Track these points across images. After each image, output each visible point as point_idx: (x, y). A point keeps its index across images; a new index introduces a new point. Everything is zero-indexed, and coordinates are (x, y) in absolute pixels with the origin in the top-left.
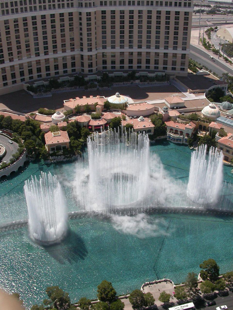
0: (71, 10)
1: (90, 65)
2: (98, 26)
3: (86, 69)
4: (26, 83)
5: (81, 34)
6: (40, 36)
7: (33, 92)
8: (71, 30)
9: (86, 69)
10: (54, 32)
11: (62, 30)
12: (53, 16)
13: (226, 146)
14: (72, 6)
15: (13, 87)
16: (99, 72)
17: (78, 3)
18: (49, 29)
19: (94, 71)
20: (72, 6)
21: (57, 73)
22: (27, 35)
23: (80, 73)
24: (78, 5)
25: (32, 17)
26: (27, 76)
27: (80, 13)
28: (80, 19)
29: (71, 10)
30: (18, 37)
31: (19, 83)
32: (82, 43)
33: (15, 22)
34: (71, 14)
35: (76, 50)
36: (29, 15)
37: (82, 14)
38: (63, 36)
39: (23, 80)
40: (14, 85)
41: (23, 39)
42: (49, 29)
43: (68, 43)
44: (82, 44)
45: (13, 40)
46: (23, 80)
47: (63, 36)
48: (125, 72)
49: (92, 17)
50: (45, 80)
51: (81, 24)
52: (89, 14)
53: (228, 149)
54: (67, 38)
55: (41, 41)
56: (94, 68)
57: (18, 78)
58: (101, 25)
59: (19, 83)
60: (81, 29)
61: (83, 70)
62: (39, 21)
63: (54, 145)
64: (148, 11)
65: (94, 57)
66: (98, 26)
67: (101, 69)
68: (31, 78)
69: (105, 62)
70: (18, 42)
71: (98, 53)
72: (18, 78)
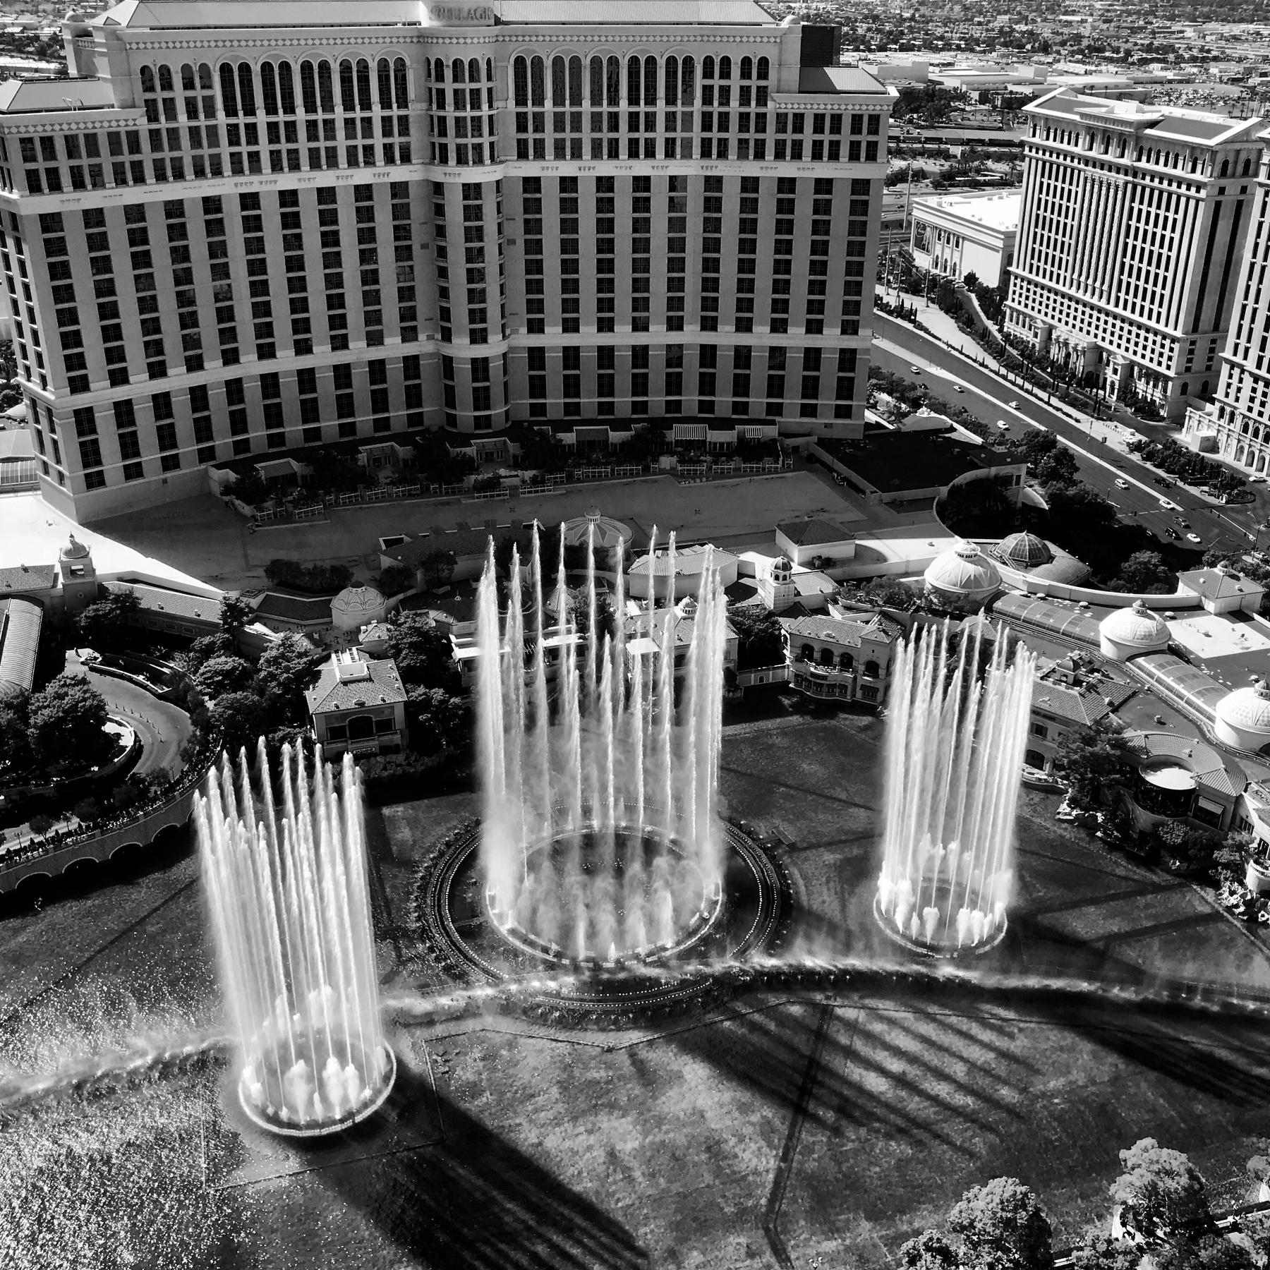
0: (399, 173)
1: (482, 399)
2: (512, 242)
3: (466, 413)
4: (219, 467)
5: (443, 273)
7: (249, 504)
8: (403, 253)
10: (332, 260)
15: (165, 481)
16: (517, 424)
17: (429, 147)
20: (406, 158)
22: (221, 271)
23: (441, 428)
24: (429, 153)
25: (242, 196)
26: (223, 441)
27: (438, 188)
28: (440, 210)
29: (399, 173)
30: (183, 277)
34: (399, 189)
35: (422, 337)
36: (227, 187)
38: (370, 277)
39: (206, 455)
40: (169, 475)
44: (445, 314)
46: (206, 455)
47: (370, 277)
49: (488, 203)
50: (294, 454)
51: (441, 231)
52: (472, 191)
56: (497, 411)
57: (187, 447)
60: (442, 253)
61: (452, 420)
62: (271, 213)
63: (345, 714)
64: (707, 179)
65: (495, 366)
66: (512, 242)
67: (525, 415)
68: (241, 447)
69: (538, 387)
70: (185, 299)
71: (512, 349)
72: (187, 447)
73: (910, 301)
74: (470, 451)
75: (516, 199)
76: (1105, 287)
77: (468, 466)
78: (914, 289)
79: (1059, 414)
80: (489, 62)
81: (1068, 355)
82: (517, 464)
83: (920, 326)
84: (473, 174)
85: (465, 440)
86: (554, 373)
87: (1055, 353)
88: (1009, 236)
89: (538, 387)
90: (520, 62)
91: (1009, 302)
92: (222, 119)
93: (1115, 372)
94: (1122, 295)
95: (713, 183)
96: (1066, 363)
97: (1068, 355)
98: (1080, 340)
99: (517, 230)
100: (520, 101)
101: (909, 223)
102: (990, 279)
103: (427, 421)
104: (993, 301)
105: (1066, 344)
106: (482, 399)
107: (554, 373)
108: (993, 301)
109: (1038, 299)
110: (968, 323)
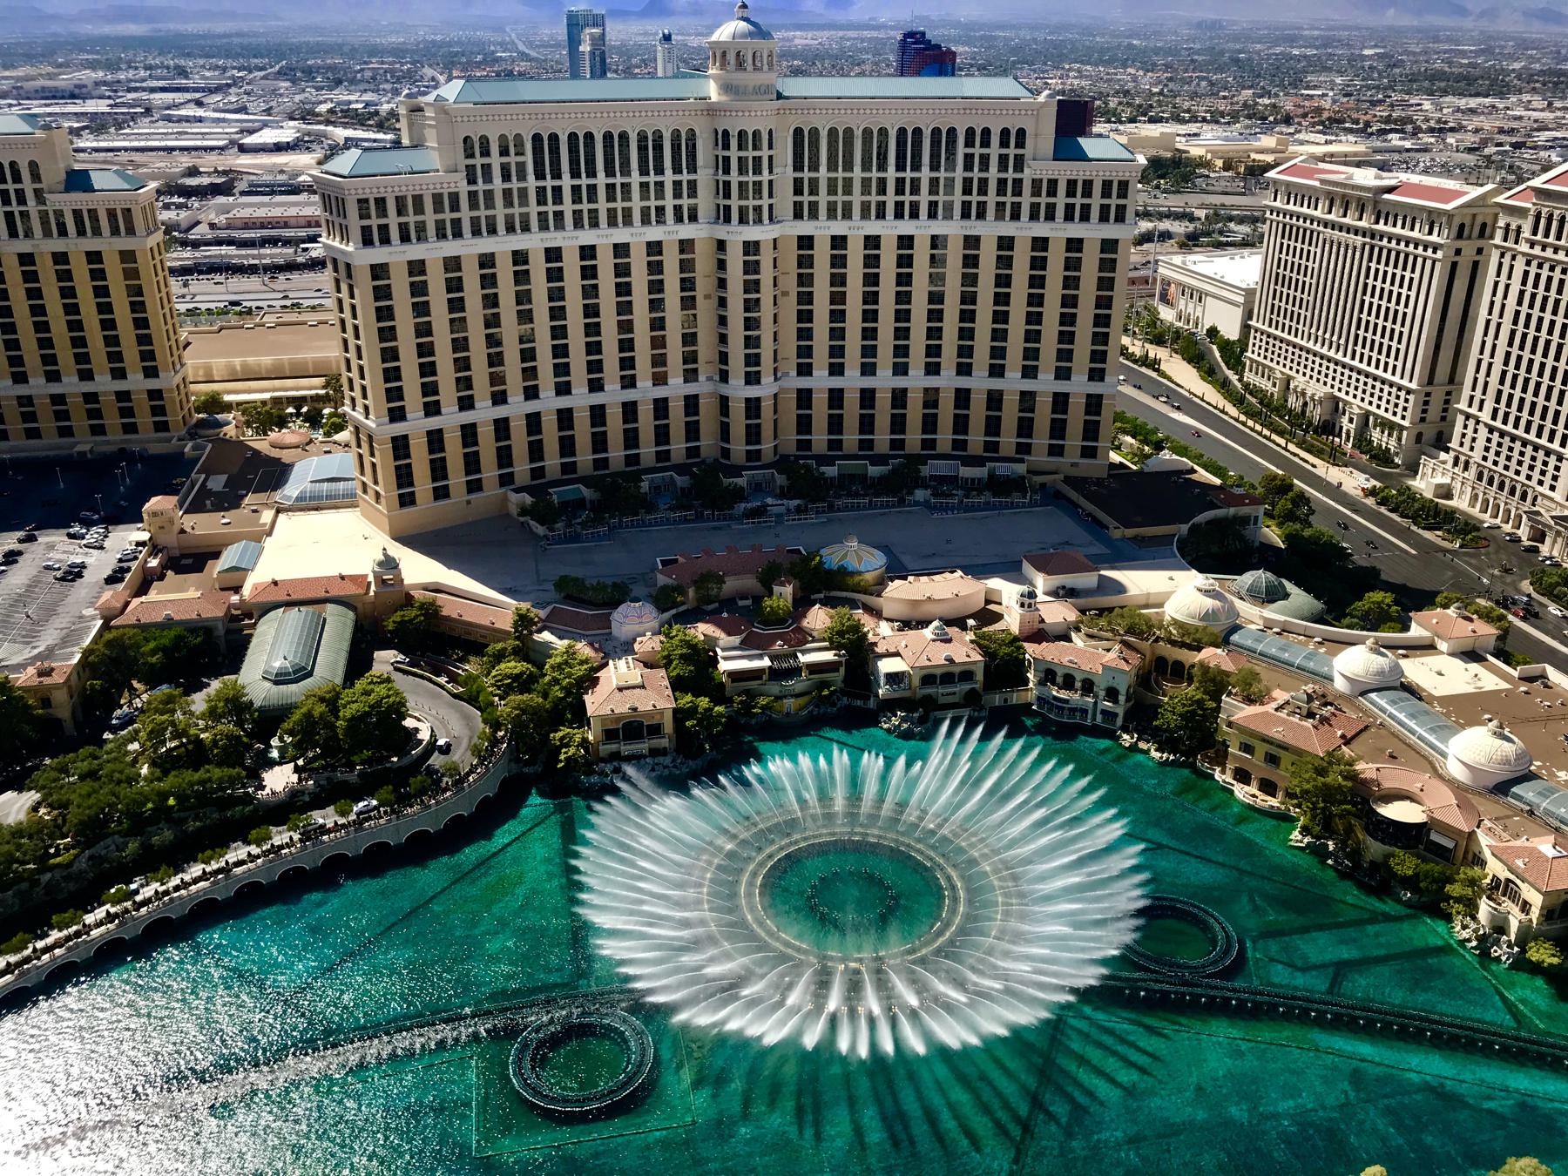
1: (753, 434)
2: (785, 294)
3: (739, 447)
4: (517, 491)
5: (723, 321)
6: (575, 321)
8: (688, 303)
9: (739, 447)
10: (625, 308)
11: (656, 305)
12: (621, 250)
13: (1266, 740)
14: (693, 218)
15: (469, 502)
16: (785, 458)
18: (607, 299)
20: (693, 218)
21: (632, 460)
22: (525, 317)
23: (716, 460)
24: (714, 213)
25: (547, 250)
26: (521, 467)
28: (722, 265)
29: (687, 231)
30: (492, 322)
31: (492, 490)
32: (726, 354)
33: (482, 266)
34: (686, 246)
35: (702, 378)
36: (534, 242)
38: (658, 324)
39: (506, 480)
40: (473, 496)
41: (510, 329)
42: (607, 299)
43: (675, 350)
44: (724, 358)
47: (658, 324)
49: (766, 259)
50: (584, 480)
51: (722, 284)
52: (751, 247)
53: (1274, 750)
54: (674, 334)
55: (576, 340)
56: (767, 446)
57: (490, 471)
59: (492, 490)
60: (722, 302)
61: (726, 453)
62: (572, 265)
64: (966, 238)
65: (767, 405)
66: (785, 294)
67: (792, 449)
68: (537, 473)
69: (804, 424)
70: (493, 341)
71: (782, 390)
72: (490, 471)
73: (1154, 351)
74: (741, 481)
75: (791, 254)
76: (1342, 341)
77: (738, 495)
78: (1159, 341)
79: (1296, 460)
80: (770, 132)
81: (1305, 404)
82: (784, 494)
84: (752, 233)
85: (737, 471)
86: (820, 411)
87: (1293, 402)
88: (1249, 293)
89: (804, 424)
90: (798, 132)
91: (1249, 354)
92: (532, 183)
93: (1351, 421)
94: (1359, 349)
95: (972, 242)
96: (1304, 412)
97: (1305, 404)
98: (1317, 390)
99: (790, 284)
100: (798, 167)
101: (1155, 280)
102: (1231, 332)
103: (704, 453)
104: (1234, 353)
105: (1303, 394)
106: (753, 434)
107: (820, 411)
108: (1234, 353)
110: (1209, 373)
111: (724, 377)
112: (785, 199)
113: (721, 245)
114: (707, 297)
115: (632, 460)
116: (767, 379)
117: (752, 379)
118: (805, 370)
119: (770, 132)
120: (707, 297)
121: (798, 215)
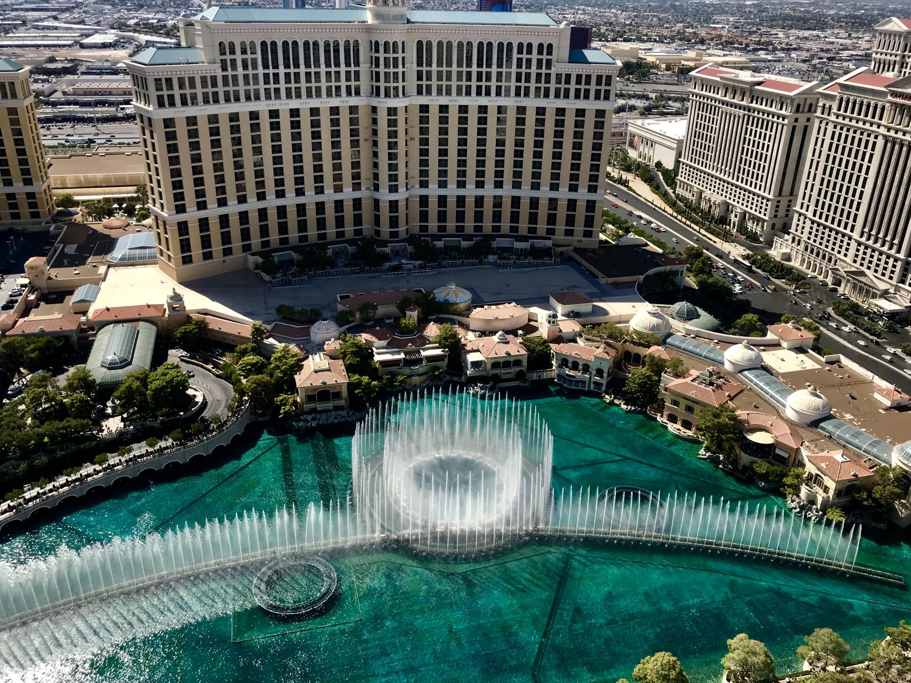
1: (394, 222)
2: (413, 139)
3: (385, 229)
4: (253, 254)
5: (375, 154)
6: (287, 153)
8: (355, 144)
9: (385, 229)
10: (317, 146)
12: (315, 112)
13: (686, 398)
14: (358, 93)
15: (224, 261)
16: (412, 236)
19: (403, 235)
20: (358, 93)
21: (322, 237)
22: (258, 151)
23: (372, 237)
24: (370, 91)
25: (270, 111)
26: (256, 241)
28: (375, 121)
29: (354, 101)
30: (238, 154)
31: (238, 254)
33: (231, 120)
34: (353, 110)
35: (363, 188)
36: (263, 106)
37: (379, 111)
38: (337, 156)
39: (247, 248)
40: (227, 258)
41: (248, 158)
43: (347, 172)
44: (376, 176)
45: (228, 160)
47: (337, 156)
48: (468, 238)
49: (401, 117)
50: (293, 248)
51: (375, 132)
52: (392, 111)
53: (690, 404)
55: (288, 166)
56: (402, 229)
57: (237, 243)
58: (417, 136)
59: (238, 254)
60: (375, 144)
61: (378, 233)
63: (314, 388)
64: (518, 108)
65: (402, 206)
66: (413, 139)
67: (417, 231)
68: (265, 244)
69: (424, 216)
70: (238, 165)
71: (410, 195)
72: (237, 243)
73: (626, 176)
74: (387, 250)
75: (415, 116)
76: (732, 171)
77: (385, 257)
78: (628, 169)
79: (705, 238)
80: (403, 43)
81: (710, 207)
82: (412, 257)
83: (630, 189)
84: (392, 103)
85: (384, 243)
86: (433, 209)
87: (704, 205)
88: (680, 142)
89: (424, 216)
90: (420, 43)
91: (679, 177)
92: (261, 71)
93: (736, 216)
94: (741, 175)
95: (521, 110)
96: (709, 211)
97: (710, 207)
98: (717, 198)
99: (415, 133)
100: (420, 64)
101: (626, 134)
102: (669, 165)
103: (365, 233)
104: (671, 177)
105: (710, 200)
106: (394, 222)
107: (433, 209)
108: (671, 177)
109: (710, 182)
110: (657, 188)
111: (376, 188)
112: (412, 83)
113: (374, 109)
114: (366, 140)
115: (322, 237)
116: (402, 189)
117: (394, 189)
118: (424, 184)
119: (403, 43)
120: (366, 140)
121: (420, 92)
